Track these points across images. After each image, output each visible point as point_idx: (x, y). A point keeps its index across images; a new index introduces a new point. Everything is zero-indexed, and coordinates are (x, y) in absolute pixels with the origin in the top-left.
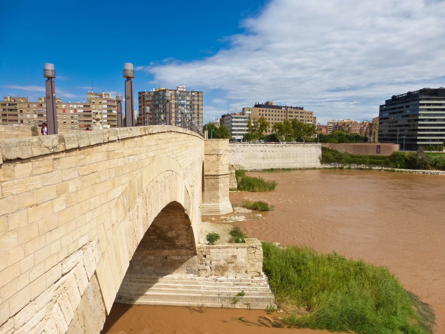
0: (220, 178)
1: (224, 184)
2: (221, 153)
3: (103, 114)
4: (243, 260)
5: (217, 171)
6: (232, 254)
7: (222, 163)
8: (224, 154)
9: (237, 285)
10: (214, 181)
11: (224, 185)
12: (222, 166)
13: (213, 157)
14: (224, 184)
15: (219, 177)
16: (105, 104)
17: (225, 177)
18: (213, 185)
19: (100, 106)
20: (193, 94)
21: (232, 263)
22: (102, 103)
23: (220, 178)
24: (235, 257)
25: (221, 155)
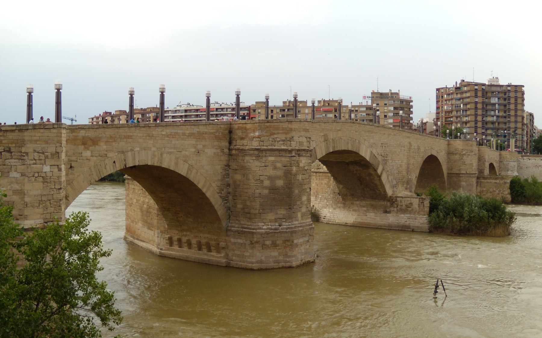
0: (462, 177)
2: (464, 152)
3: (388, 119)
4: (417, 206)
5: (460, 170)
6: (409, 202)
7: (465, 162)
8: (468, 154)
9: (409, 219)
12: (465, 166)
13: (456, 157)
15: (461, 175)
16: (391, 105)
17: (468, 177)
19: (386, 108)
22: (387, 105)
23: (462, 177)
24: (411, 204)
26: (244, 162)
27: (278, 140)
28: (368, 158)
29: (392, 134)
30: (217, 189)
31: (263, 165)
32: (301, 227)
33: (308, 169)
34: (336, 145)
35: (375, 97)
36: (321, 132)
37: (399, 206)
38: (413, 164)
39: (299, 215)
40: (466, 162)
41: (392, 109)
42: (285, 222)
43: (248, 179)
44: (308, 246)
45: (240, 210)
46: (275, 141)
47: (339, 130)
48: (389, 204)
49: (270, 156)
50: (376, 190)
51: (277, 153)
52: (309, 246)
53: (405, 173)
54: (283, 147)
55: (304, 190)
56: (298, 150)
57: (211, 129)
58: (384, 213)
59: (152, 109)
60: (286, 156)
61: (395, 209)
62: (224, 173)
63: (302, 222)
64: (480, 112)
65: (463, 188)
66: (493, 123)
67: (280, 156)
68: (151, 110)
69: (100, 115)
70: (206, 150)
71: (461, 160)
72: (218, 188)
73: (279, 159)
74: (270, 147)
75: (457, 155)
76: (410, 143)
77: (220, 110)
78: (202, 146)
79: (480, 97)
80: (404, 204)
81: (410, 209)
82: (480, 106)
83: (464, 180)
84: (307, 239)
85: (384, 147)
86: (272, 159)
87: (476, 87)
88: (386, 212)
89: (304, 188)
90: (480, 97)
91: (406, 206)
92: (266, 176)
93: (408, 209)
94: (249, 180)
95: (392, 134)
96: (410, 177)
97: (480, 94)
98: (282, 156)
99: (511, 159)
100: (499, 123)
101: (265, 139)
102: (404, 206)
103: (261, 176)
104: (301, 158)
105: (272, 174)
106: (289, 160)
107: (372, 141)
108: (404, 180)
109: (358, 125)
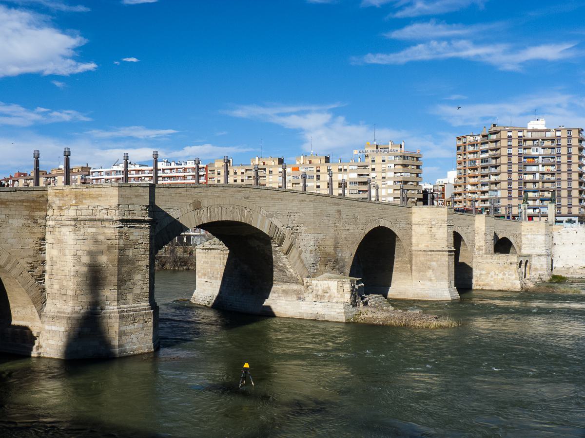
1: (439, 263)
2: (433, 223)
3: (387, 180)
4: (335, 291)
6: (327, 286)
7: (435, 236)
10: (423, 259)
11: (438, 265)
13: (423, 228)
14: (439, 263)
16: (390, 162)
18: (422, 264)
20: (558, 134)
21: (327, 293)
24: (329, 288)
25: (433, 226)
26: (60, 235)
27: (100, 208)
28: (266, 231)
29: (308, 200)
30: (27, 266)
31: (81, 237)
32: (133, 311)
33: (142, 243)
34: (213, 215)
35: (369, 151)
36: (189, 199)
37: (314, 291)
38: (346, 238)
39: (130, 297)
40: (436, 236)
41: (392, 166)
42: (109, 305)
43: (65, 255)
44: (143, 335)
45: (56, 291)
46: (97, 210)
47: (218, 196)
48: (302, 288)
49: (89, 227)
50: (286, 271)
51: (99, 223)
52: (145, 335)
53: (332, 251)
54: (106, 217)
55: (137, 267)
56: (127, 221)
57: (19, 197)
58: (297, 300)
59: (80, 170)
60: (110, 228)
61: (310, 295)
62: (39, 248)
63: (133, 305)
64: (515, 168)
65: (433, 270)
66: (534, 183)
67: (102, 227)
68: (78, 171)
69: (11, 177)
70: (10, 221)
71: (429, 233)
72: (29, 265)
73: (101, 230)
74: (88, 217)
75: (424, 226)
76: (339, 211)
77: (169, 171)
78: (4, 216)
79: (515, 147)
80: (320, 289)
81: (328, 295)
82: (515, 160)
83: (434, 259)
84: (141, 326)
85: (293, 217)
86: (93, 230)
87: (510, 134)
88: (299, 299)
89: (137, 264)
90: (515, 147)
91: (323, 290)
92: (86, 250)
93: (325, 294)
94: (65, 256)
95: (308, 200)
96: (340, 255)
97: (515, 143)
98: (105, 227)
99: (538, 232)
100: (543, 182)
101: (84, 208)
102: (320, 290)
103: (78, 251)
104: (132, 230)
105: (92, 248)
106: (114, 232)
107: (272, 210)
108: (328, 258)
109: (249, 190)
